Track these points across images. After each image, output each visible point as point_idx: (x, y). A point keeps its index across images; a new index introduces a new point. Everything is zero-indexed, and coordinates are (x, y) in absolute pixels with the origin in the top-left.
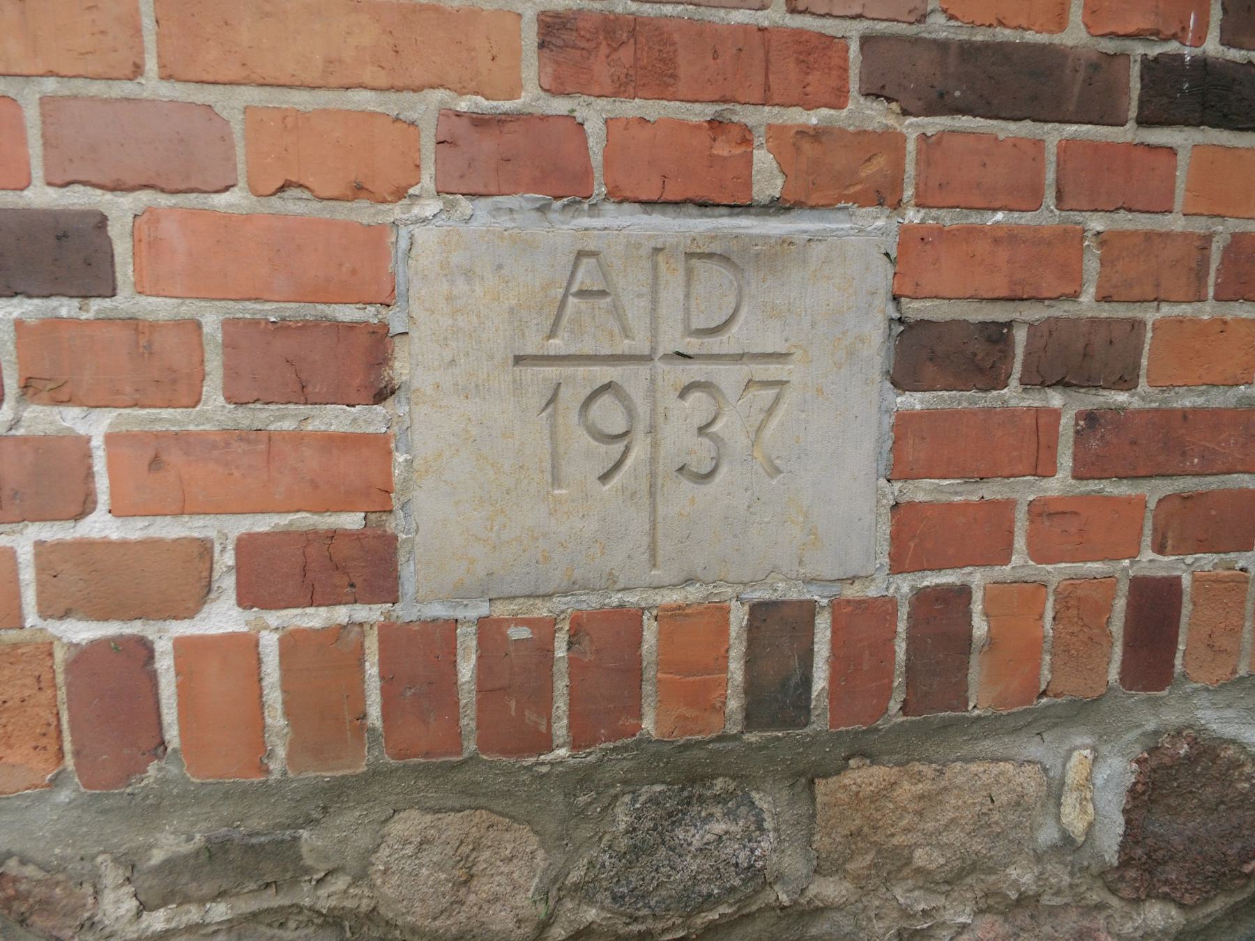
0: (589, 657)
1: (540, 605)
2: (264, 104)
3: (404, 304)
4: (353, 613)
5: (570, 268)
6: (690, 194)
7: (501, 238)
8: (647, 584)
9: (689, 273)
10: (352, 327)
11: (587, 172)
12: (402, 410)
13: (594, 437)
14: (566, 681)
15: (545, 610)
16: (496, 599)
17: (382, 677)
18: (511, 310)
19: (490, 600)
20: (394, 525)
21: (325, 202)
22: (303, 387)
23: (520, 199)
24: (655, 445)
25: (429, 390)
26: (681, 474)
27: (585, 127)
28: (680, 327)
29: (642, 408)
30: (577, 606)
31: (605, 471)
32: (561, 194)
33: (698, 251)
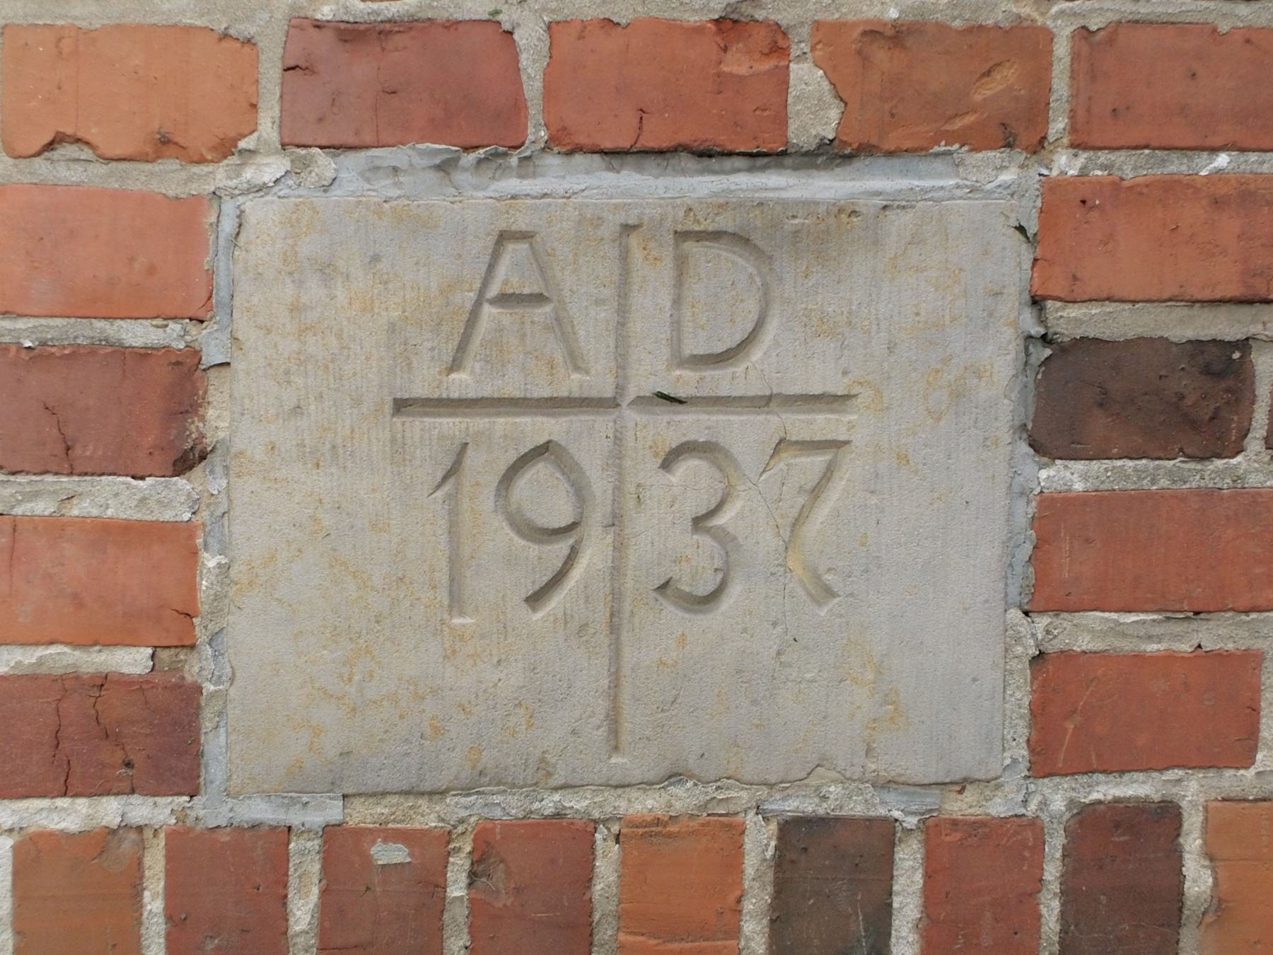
0: (505, 900)
1: (424, 808)
2: (31, 21)
3: (226, 319)
4: (127, 809)
5: (487, 259)
6: (684, 138)
7: (379, 213)
8: (603, 780)
9: (681, 265)
10: (145, 354)
11: (518, 106)
12: (217, 484)
13: (520, 532)
14: (465, 940)
15: (433, 816)
16: (354, 795)
17: (169, 917)
18: (392, 328)
19: (344, 796)
20: (196, 669)
21: (113, 164)
22: (68, 449)
23: (411, 152)
24: (620, 547)
25: (259, 454)
26: (664, 595)
27: (516, 37)
28: (665, 352)
29: (600, 484)
30: (486, 813)
31: (537, 587)
32: (475, 142)
33: (697, 228)
